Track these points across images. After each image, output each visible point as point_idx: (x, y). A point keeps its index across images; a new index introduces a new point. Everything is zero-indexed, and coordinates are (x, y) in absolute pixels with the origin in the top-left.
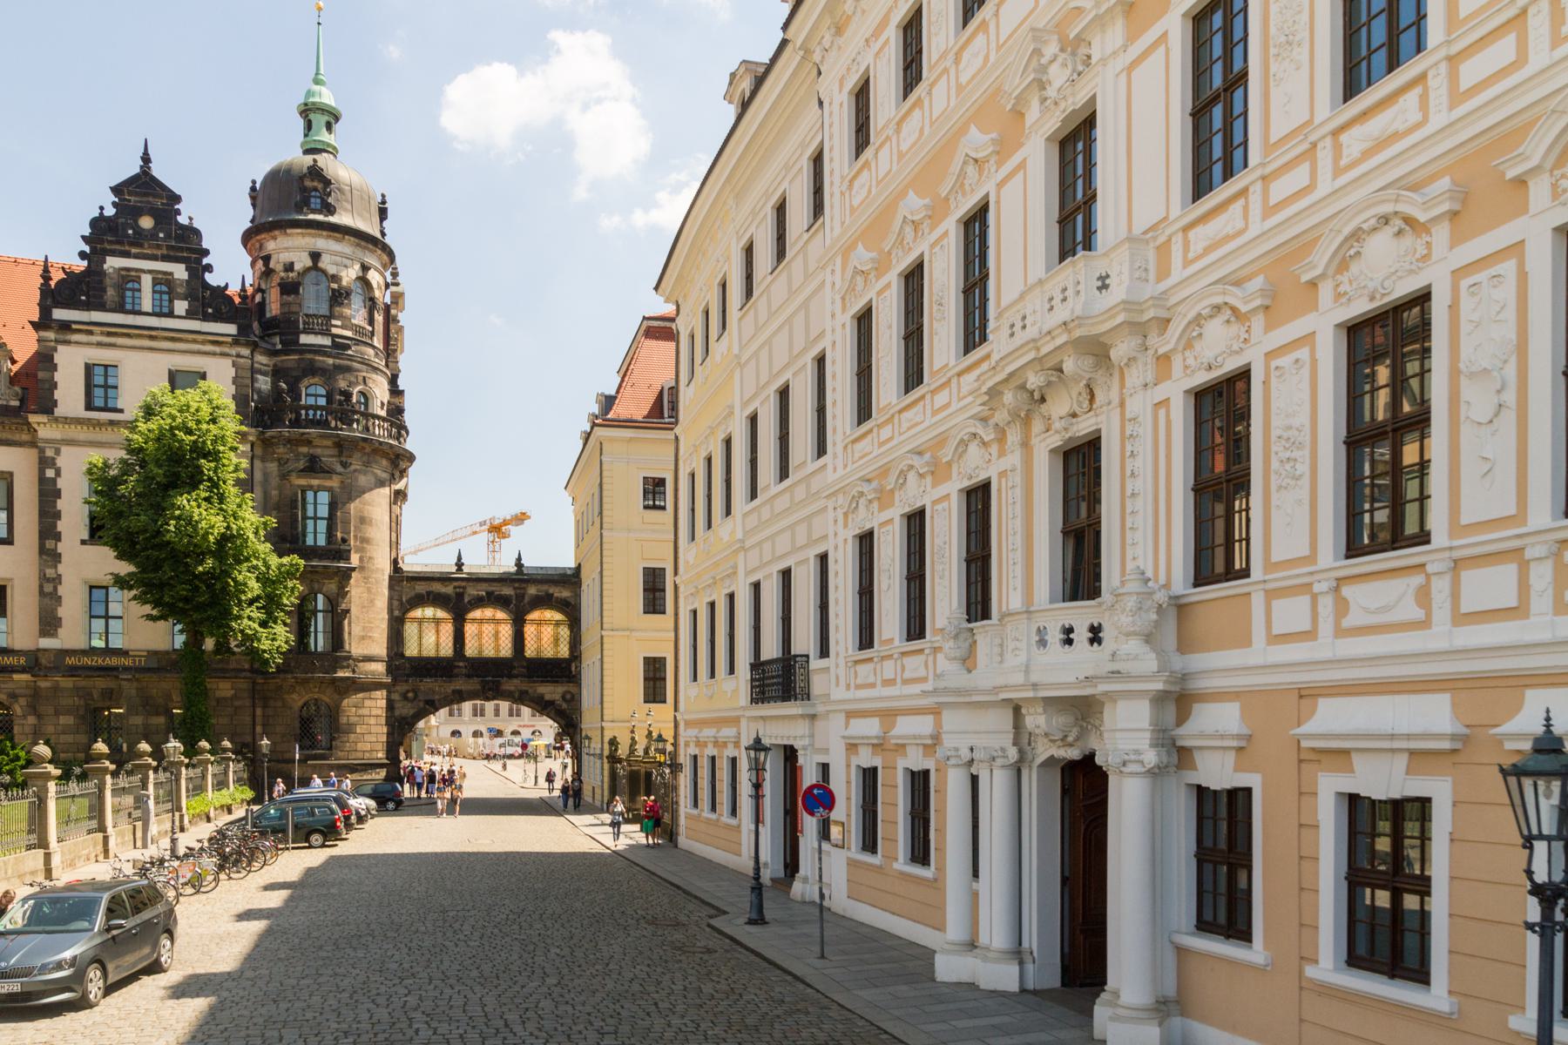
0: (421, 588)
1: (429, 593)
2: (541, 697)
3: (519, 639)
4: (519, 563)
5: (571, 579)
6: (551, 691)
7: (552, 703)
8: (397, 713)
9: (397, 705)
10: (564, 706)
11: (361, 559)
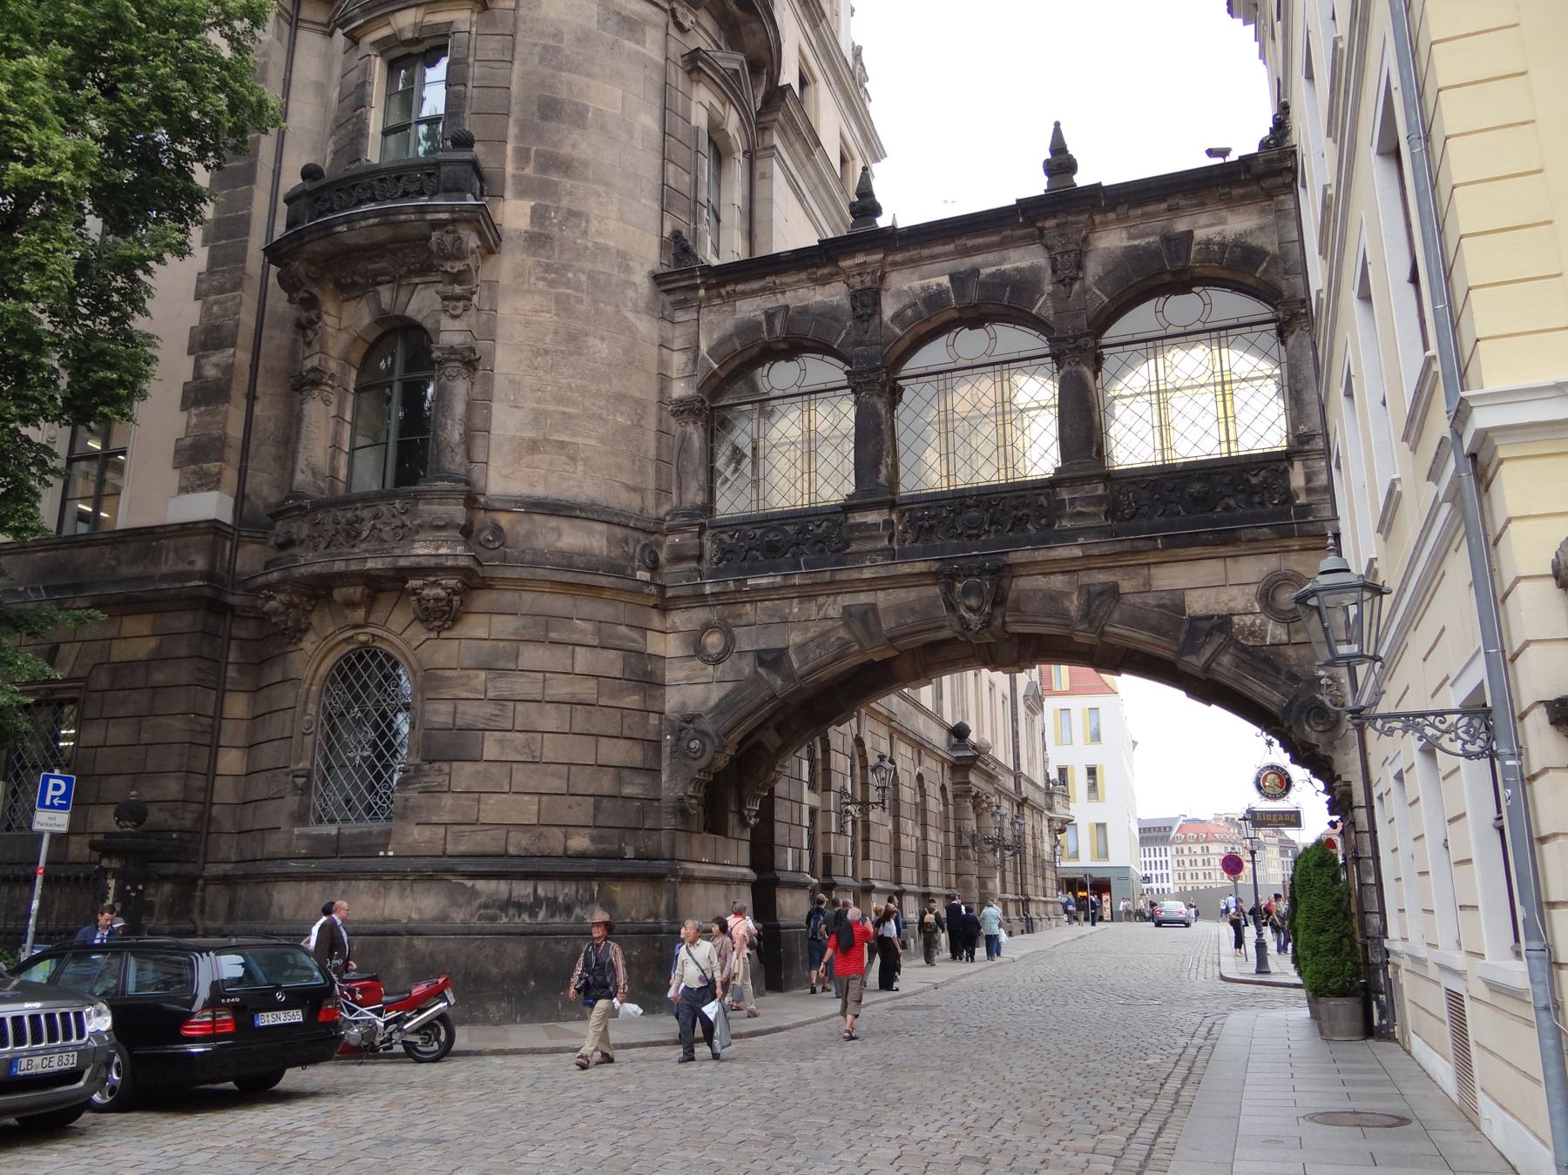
0: (750, 308)
2: (1175, 604)
3: (1082, 424)
4: (1060, 163)
5: (1267, 173)
6: (1219, 585)
7: (1222, 624)
8: (673, 701)
9: (673, 674)
10: (1275, 632)
11: (538, 215)
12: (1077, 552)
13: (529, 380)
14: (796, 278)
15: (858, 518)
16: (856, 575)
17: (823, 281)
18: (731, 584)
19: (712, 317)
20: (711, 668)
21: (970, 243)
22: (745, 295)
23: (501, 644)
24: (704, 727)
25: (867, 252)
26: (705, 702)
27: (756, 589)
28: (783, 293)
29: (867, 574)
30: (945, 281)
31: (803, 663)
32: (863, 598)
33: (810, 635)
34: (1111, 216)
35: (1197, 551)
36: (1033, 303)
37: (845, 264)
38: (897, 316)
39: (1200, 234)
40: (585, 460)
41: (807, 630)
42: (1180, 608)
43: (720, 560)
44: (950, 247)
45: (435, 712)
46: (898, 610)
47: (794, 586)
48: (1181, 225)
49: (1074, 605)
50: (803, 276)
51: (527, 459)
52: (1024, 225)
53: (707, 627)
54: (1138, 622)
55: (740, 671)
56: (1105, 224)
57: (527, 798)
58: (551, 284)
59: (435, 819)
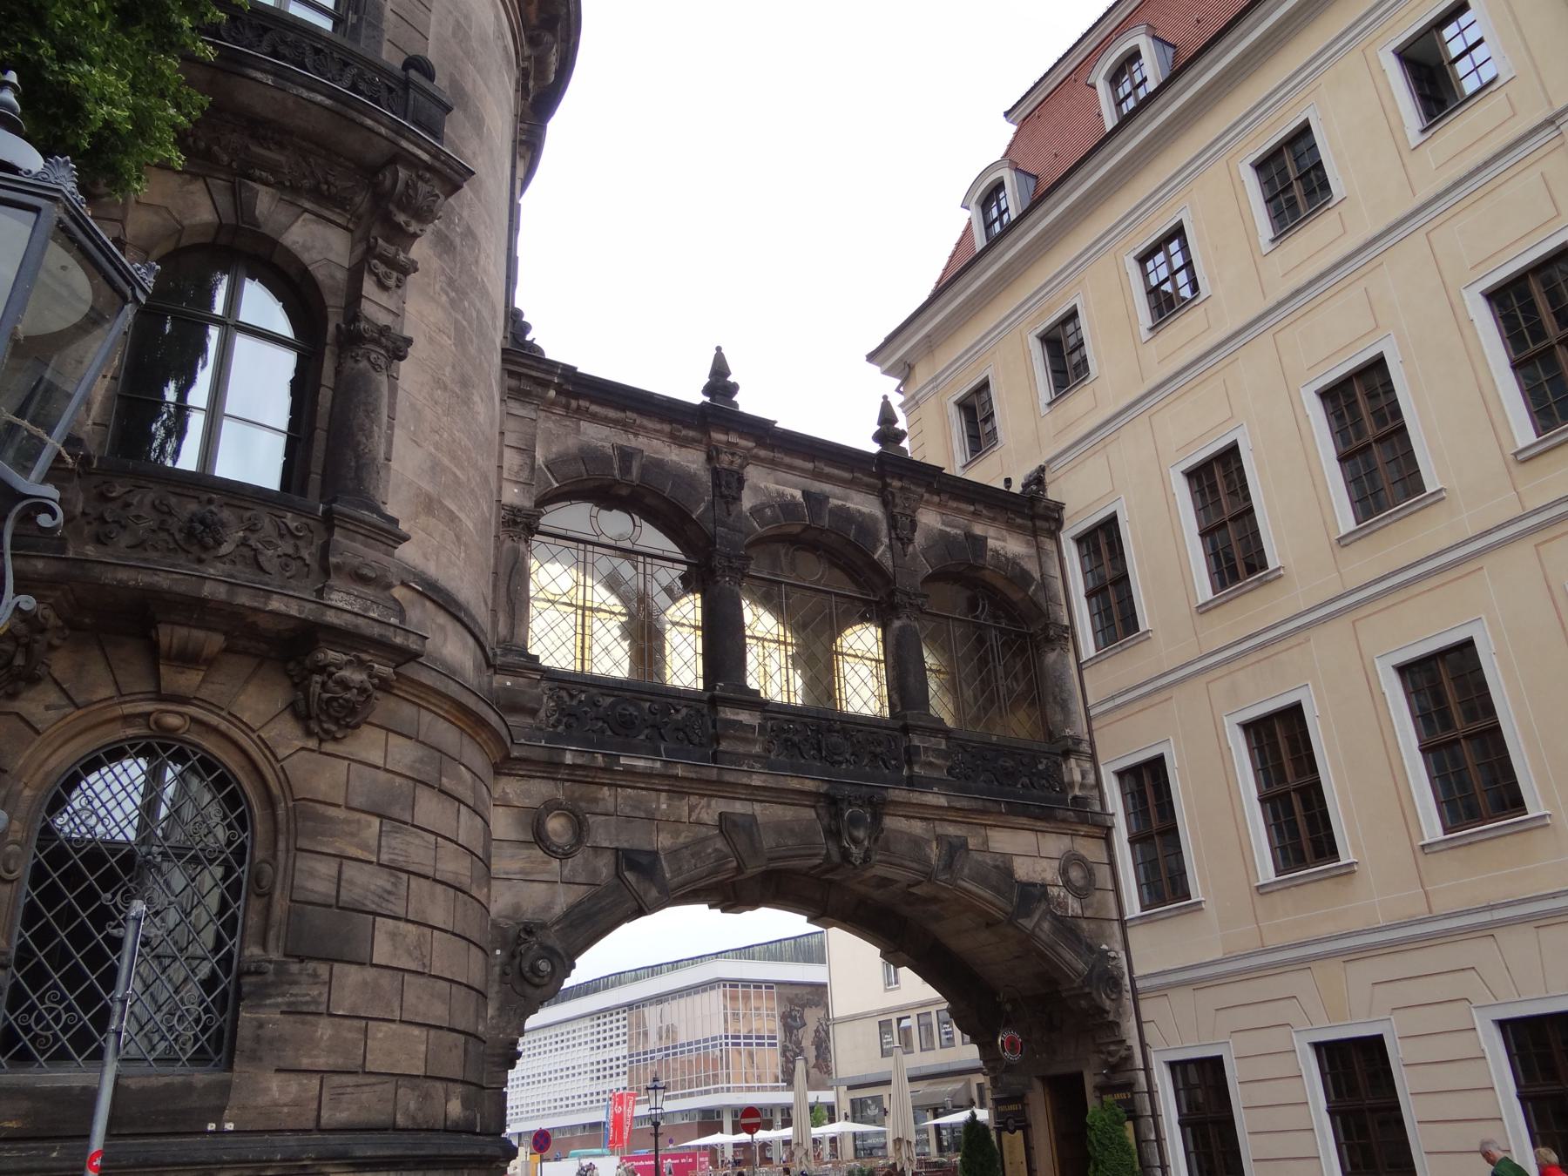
0: (598, 435)
1: (626, 455)
7: (1033, 894)
10: (1074, 906)
12: (943, 801)
13: (428, 413)
14: (658, 427)
15: (728, 714)
16: (745, 780)
17: (683, 443)
18: (600, 757)
19: (551, 425)
20: (556, 863)
21: (827, 470)
22: (595, 418)
23: (398, 780)
24: (549, 942)
25: (742, 435)
26: (548, 907)
27: (630, 771)
28: (636, 435)
29: (757, 781)
30: (798, 494)
31: (678, 871)
32: (739, 807)
33: (681, 840)
34: (936, 499)
35: (1024, 821)
36: (876, 548)
37: (718, 436)
38: (756, 511)
39: (991, 543)
40: (466, 545)
41: (677, 834)
42: (1007, 871)
43: (559, 721)
44: (810, 466)
45: (312, 874)
46: (779, 828)
47: (676, 777)
48: (978, 529)
49: (933, 852)
50: (667, 428)
51: (423, 519)
52: (871, 475)
53: (551, 806)
54: (982, 880)
55: (595, 872)
56: (928, 502)
57: (416, 1031)
58: (452, 301)
59: (305, 1063)
